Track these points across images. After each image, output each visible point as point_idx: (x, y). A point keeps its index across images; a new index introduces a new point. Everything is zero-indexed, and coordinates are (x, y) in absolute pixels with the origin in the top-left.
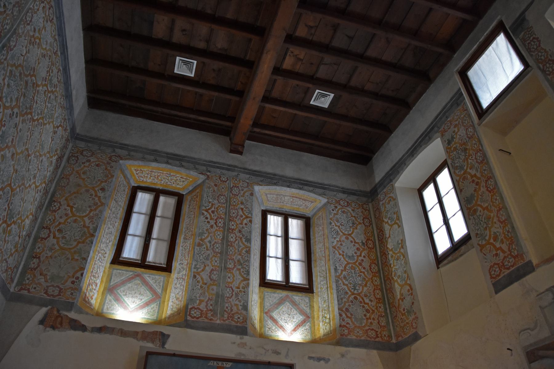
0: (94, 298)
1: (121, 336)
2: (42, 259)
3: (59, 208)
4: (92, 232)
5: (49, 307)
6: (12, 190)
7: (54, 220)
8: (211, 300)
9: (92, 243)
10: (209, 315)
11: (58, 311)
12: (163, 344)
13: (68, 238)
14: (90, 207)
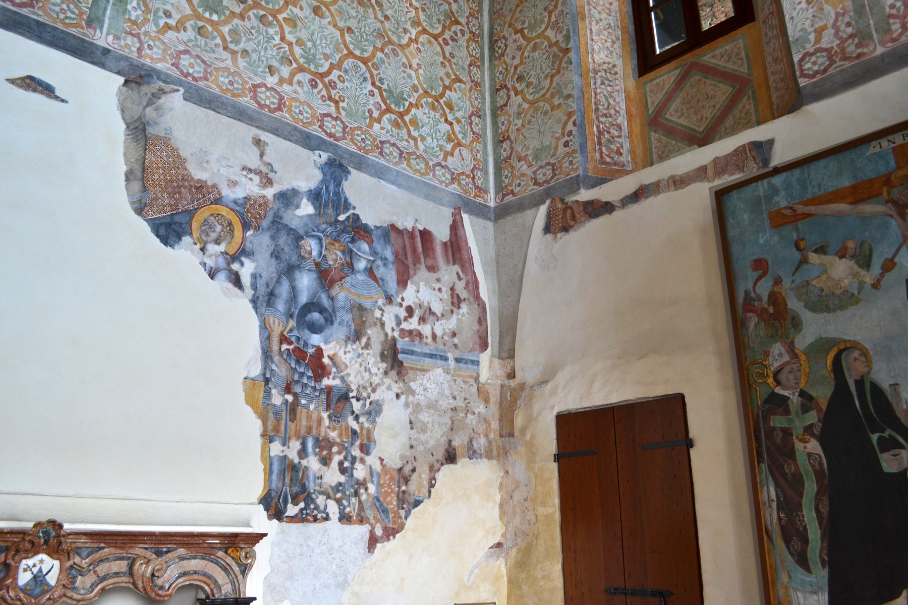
0: (624, 151)
1: (676, 189)
2: (513, 137)
3: (506, 46)
4: (563, 45)
5: (548, 202)
6: (365, 61)
7: (506, 70)
8: (843, 15)
9: (571, 63)
10: (852, 48)
11: (562, 200)
12: (766, 162)
13: (534, 81)
14: (546, 9)
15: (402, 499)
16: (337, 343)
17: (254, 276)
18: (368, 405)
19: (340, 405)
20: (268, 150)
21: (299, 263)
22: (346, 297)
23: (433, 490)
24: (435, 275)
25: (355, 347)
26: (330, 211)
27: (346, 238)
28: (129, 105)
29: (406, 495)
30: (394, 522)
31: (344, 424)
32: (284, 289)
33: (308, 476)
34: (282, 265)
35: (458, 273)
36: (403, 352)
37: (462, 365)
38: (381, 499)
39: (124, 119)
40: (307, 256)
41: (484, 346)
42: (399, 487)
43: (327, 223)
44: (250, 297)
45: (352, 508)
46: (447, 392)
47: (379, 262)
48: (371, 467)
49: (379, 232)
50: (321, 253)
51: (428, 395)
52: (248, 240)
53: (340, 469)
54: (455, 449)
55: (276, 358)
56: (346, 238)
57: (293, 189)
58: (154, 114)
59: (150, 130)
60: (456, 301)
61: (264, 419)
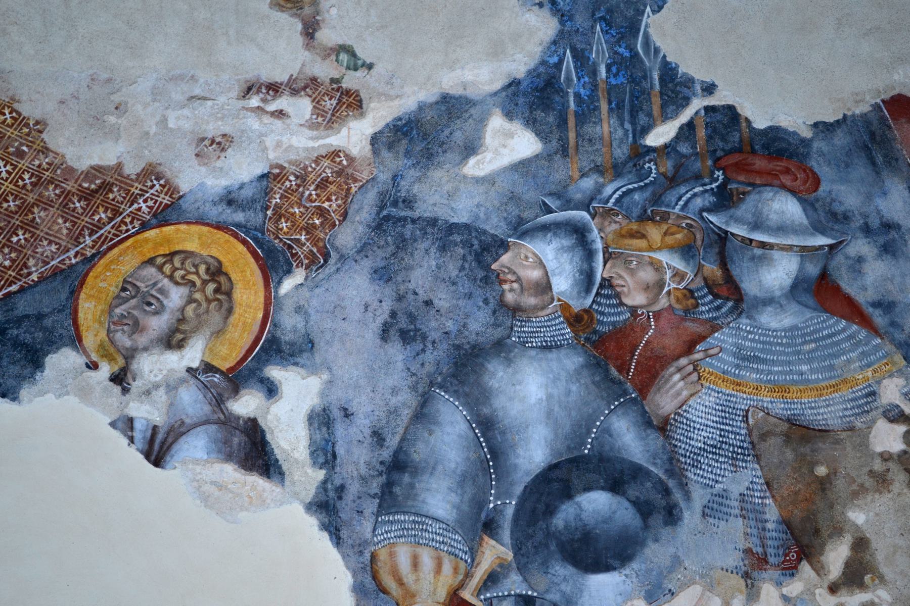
16: (711, 587)
17: (322, 420)
21: (498, 333)
22: (726, 411)
26: (607, 126)
32: (450, 435)
34: (430, 356)
40: (531, 301)
43: (598, 170)
44: (310, 492)
47: (860, 246)
49: (841, 139)
50: (587, 278)
56: (692, 199)
57: (445, 99)
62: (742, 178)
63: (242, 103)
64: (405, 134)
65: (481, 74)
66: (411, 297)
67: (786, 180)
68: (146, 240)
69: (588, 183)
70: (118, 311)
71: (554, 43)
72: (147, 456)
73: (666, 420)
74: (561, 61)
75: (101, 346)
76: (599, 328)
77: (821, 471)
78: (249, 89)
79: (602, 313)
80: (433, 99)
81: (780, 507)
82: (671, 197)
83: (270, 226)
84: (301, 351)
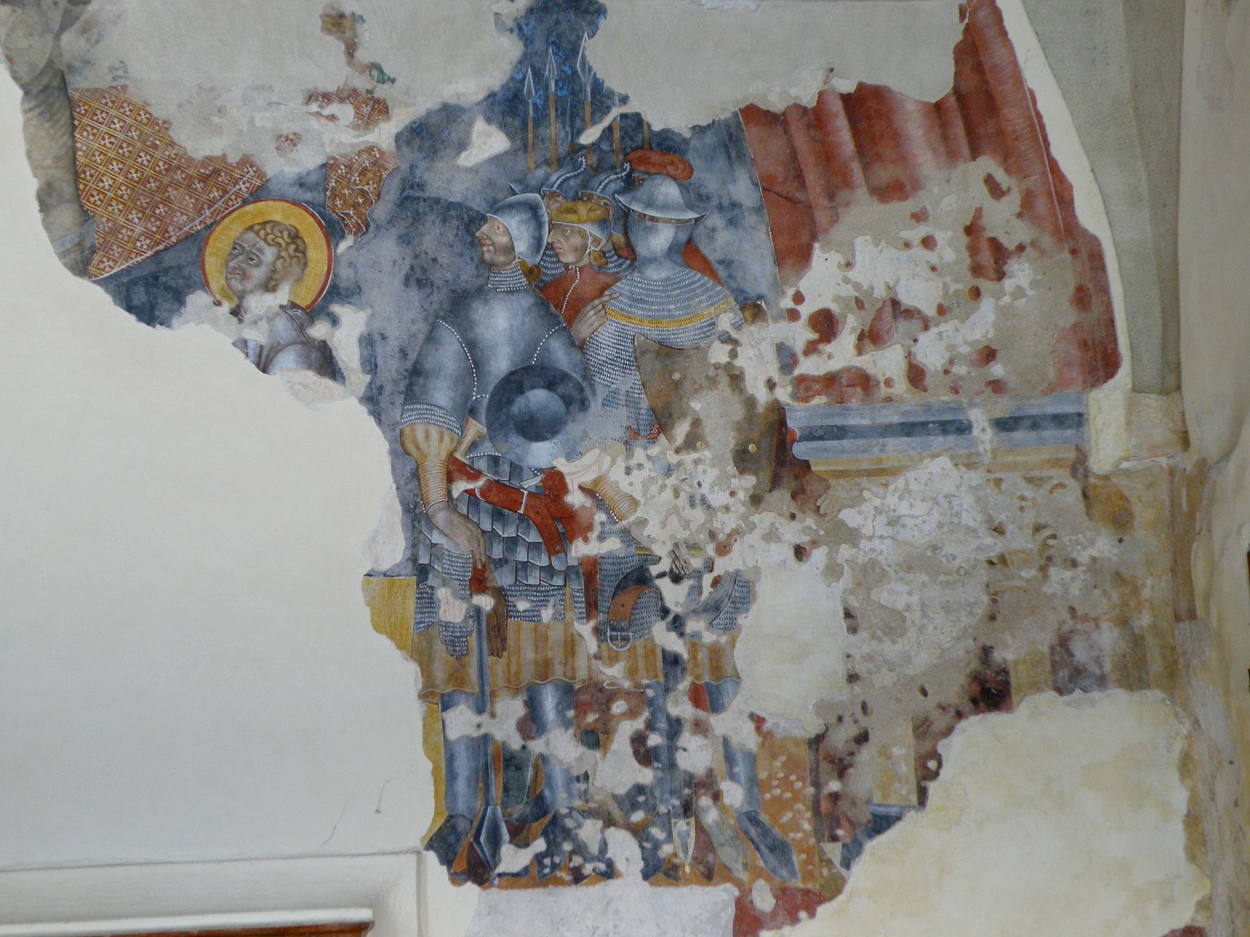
15: (829, 815)
16: (605, 450)
17: (368, 341)
18: (707, 588)
19: (627, 598)
20: (365, 34)
21: (479, 282)
22: (621, 335)
23: (932, 787)
24: (909, 206)
25: (654, 450)
26: (554, 129)
27: (609, 182)
28: (23, 43)
29: (843, 805)
30: (809, 876)
31: (639, 643)
33: (549, 778)
35: (990, 181)
36: (810, 436)
37: (1018, 435)
38: (764, 817)
39: (16, 78)
41: (1101, 361)
42: (817, 785)
43: (547, 162)
44: (362, 390)
45: (678, 842)
46: (972, 518)
47: (716, 220)
48: (726, 742)
49: (710, 139)
51: (905, 534)
52: (344, 262)
53: (636, 753)
54: (1005, 671)
55: (441, 518)
56: (609, 182)
58: (82, 43)
59: (78, 84)
60: (989, 258)
61: (423, 657)
62: (642, 168)
63: (305, 108)
64: (418, 134)
65: (470, 84)
66: (423, 256)
67: (671, 169)
68: (247, 213)
69: (540, 173)
70: (231, 264)
71: (520, 62)
72: (258, 366)
73: (584, 342)
74: (524, 78)
75: (222, 289)
76: (544, 278)
77: (677, 376)
78: (310, 97)
79: (546, 268)
80: (437, 107)
81: (649, 400)
82: (595, 182)
83: (329, 203)
84: (353, 294)
